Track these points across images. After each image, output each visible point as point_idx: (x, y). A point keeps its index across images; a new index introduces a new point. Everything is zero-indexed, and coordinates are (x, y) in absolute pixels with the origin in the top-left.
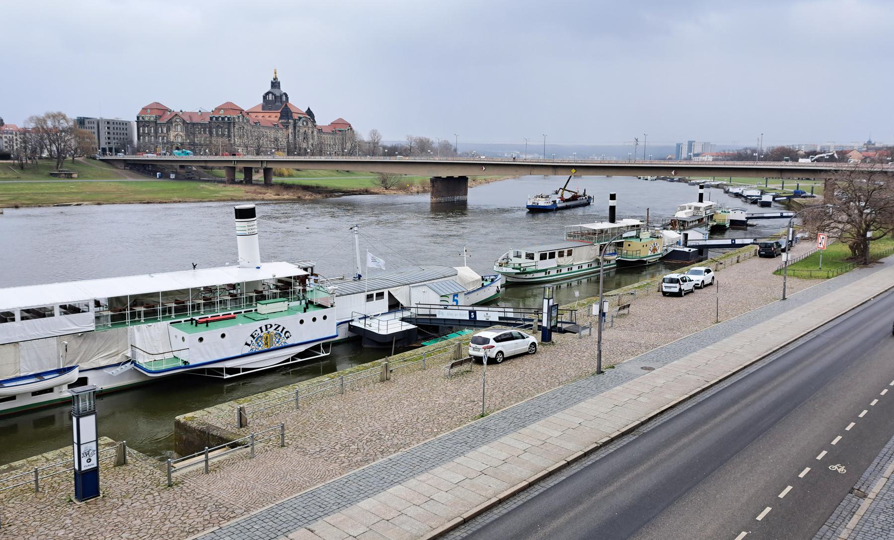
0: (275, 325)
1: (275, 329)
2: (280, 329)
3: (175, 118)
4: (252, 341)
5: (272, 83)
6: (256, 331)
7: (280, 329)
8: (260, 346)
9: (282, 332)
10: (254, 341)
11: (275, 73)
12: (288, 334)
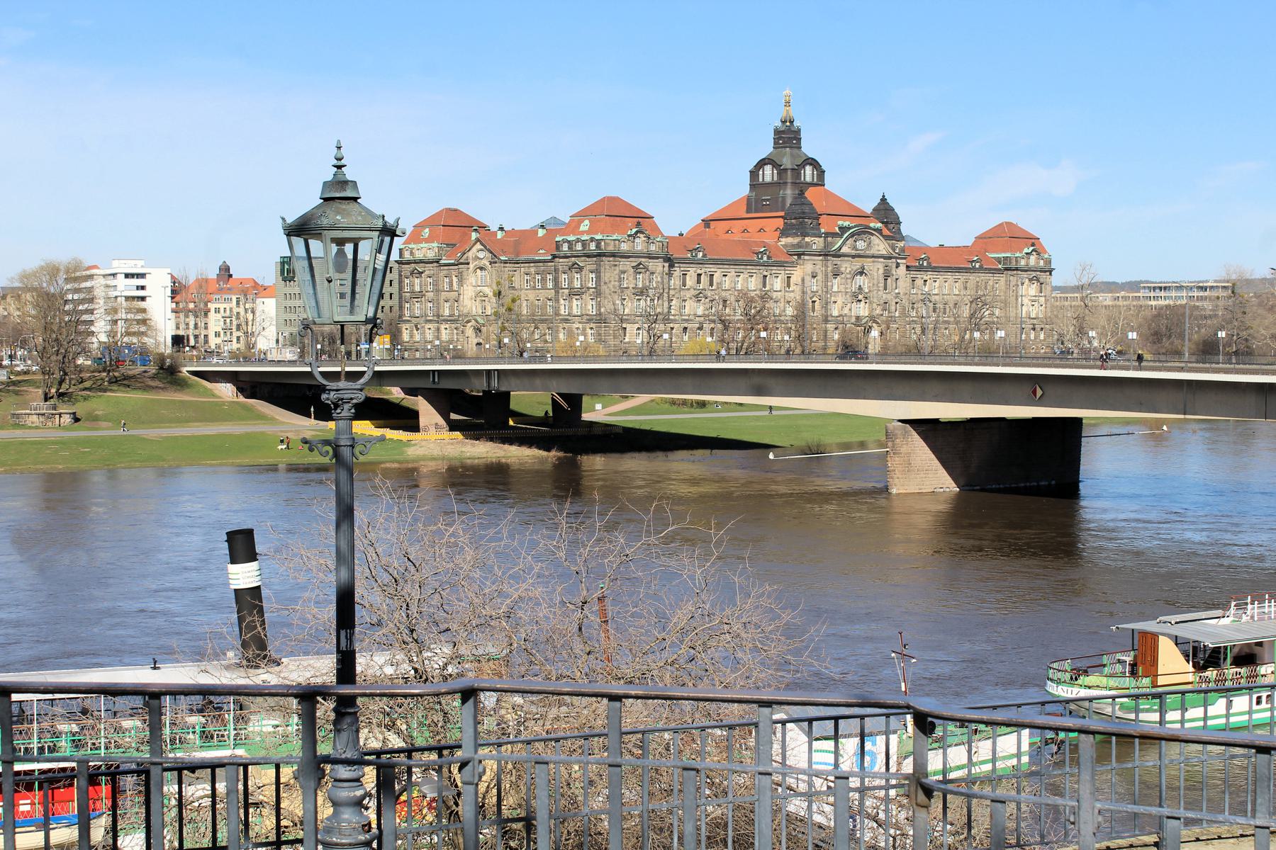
3: (474, 249)
5: (777, 132)
11: (788, 103)
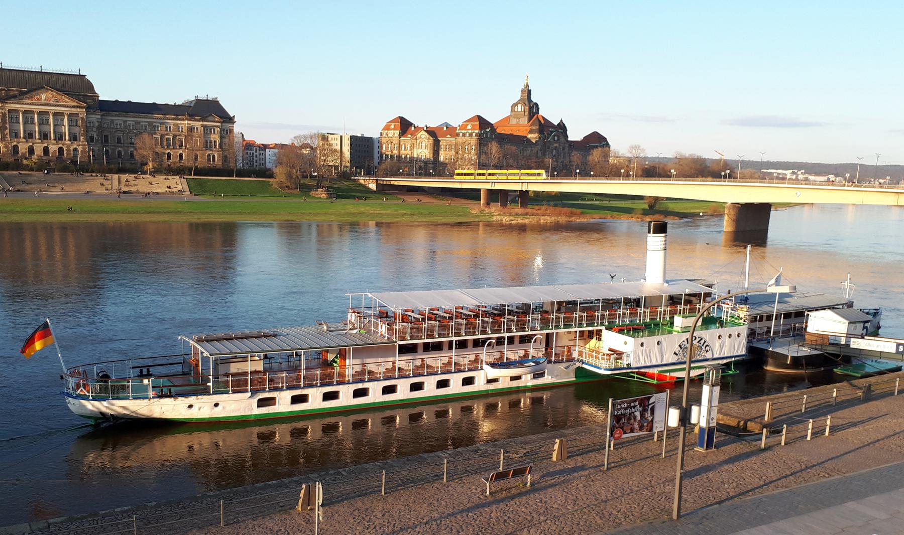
0: (699, 337)
1: (698, 342)
2: (702, 342)
4: (679, 351)
6: (684, 341)
7: (702, 342)
8: (685, 356)
9: (703, 345)
10: (681, 352)
12: (707, 348)
